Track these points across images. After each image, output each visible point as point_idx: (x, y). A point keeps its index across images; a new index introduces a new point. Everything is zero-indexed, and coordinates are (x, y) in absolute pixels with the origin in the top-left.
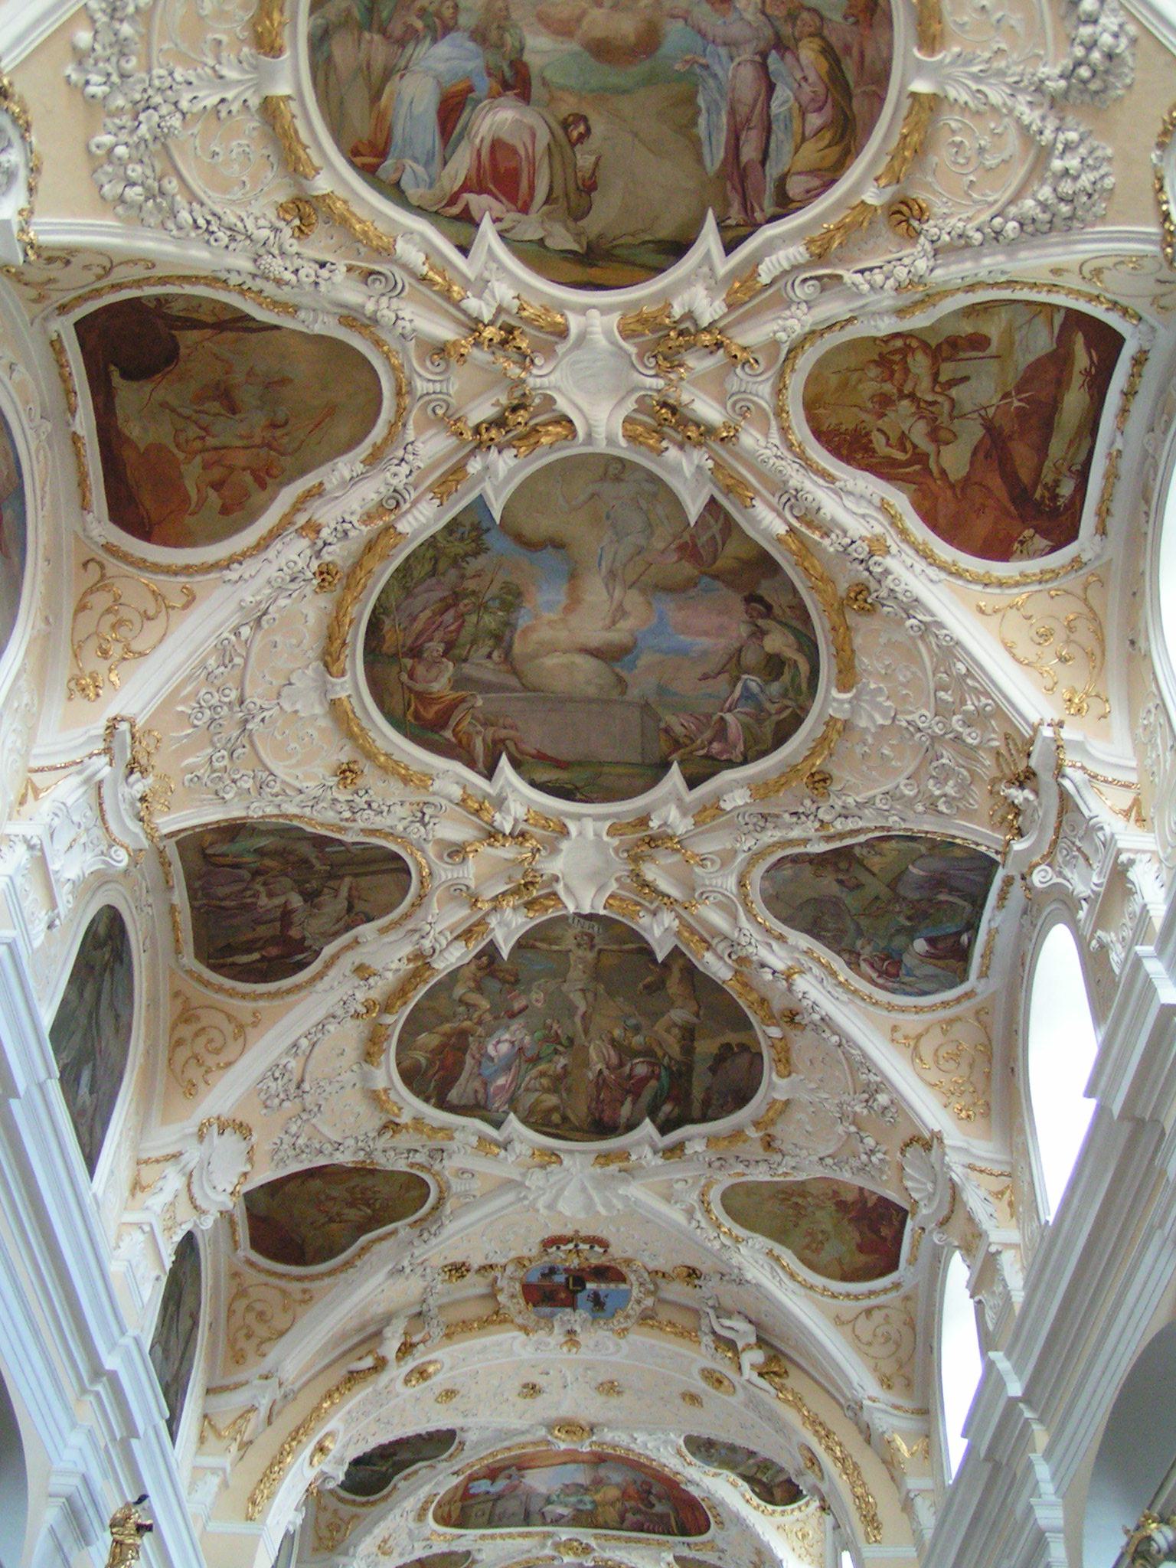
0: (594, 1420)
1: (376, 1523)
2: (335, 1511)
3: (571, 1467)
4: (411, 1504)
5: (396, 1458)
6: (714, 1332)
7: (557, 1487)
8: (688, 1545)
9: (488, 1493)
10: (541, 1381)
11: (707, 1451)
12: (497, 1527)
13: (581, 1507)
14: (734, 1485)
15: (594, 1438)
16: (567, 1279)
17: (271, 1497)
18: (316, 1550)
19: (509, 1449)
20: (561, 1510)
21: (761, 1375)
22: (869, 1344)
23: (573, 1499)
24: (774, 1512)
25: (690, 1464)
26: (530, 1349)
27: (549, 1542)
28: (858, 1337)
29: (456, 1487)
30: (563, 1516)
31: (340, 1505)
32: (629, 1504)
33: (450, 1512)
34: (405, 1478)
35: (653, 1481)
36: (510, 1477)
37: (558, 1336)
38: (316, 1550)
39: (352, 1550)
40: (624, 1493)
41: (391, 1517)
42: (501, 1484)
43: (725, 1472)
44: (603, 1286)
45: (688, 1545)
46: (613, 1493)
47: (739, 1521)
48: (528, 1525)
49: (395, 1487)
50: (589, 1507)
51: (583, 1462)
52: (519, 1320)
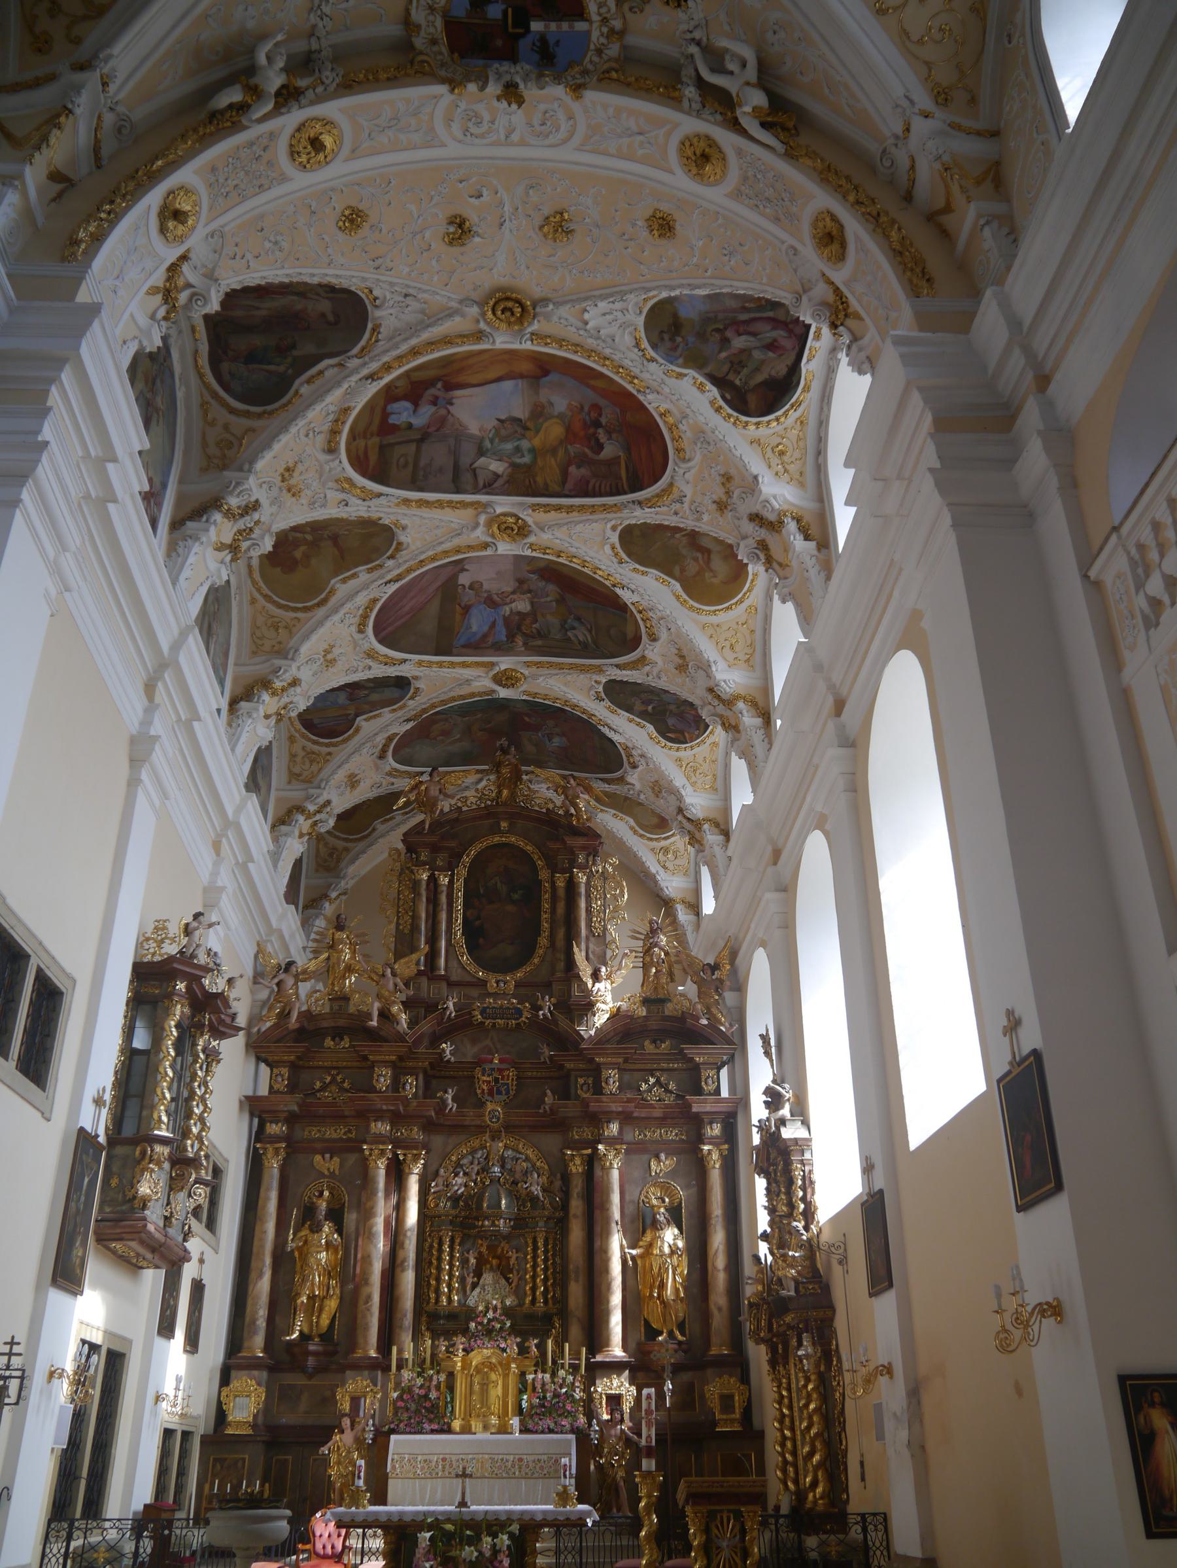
0: (537, 292)
1: (274, 437)
2: (226, 427)
3: (508, 385)
4: (318, 415)
5: (295, 353)
6: (700, 83)
7: (491, 424)
8: (640, 503)
9: (410, 426)
10: (471, 210)
11: (672, 340)
12: (421, 490)
13: (518, 461)
14: (701, 388)
15: (535, 327)
16: (505, 13)
17: (98, 239)
18: (204, 470)
19: (432, 344)
20: (497, 466)
21: (763, 125)
22: (920, 42)
23: (509, 446)
24: (747, 423)
25: (652, 360)
26: (456, 128)
27: (482, 519)
28: (907, 34)
29: (370, 406)
30: (497, 476)
31: (232, 418)
32: (572, 449)
33: (366, 447)
34: (309, 381)
35: (602, 402)
36: (434, 402)
37: (494, 88)
38: (204, 470)
39: (246, 467)
40: (568, 429)
41: (293, 430)
42: (422, 417)
43: (691, 372)
44: (553, 26)
45: (640, 503)
46: (554, 431)
47: (702, 436)
48: (458, 491)
49: (297, 392)
50: (527, 459)
51: (521, 376)
52: (443, 73)
